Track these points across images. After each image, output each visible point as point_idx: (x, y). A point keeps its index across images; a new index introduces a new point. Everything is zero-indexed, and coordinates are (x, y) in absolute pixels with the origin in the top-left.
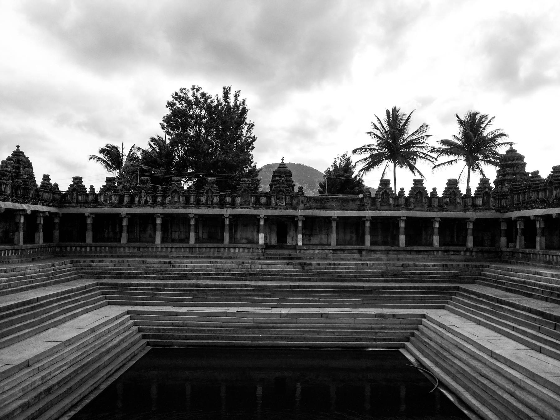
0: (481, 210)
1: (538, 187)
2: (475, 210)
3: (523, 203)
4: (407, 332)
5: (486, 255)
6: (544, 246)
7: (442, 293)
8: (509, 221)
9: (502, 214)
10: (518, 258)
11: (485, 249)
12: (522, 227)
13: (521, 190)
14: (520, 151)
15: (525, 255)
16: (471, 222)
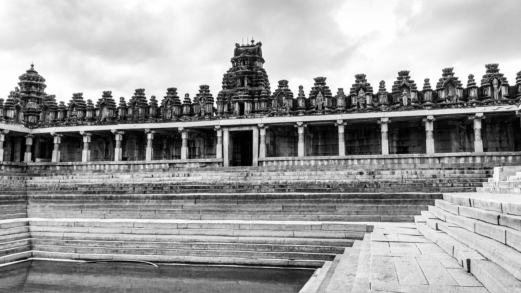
0: (12, 122)
1: (87, 107)
2: (7, 122)
3: (63, 120)
4: (24, 241)
5: (13, 169)
6: (89, 158)
7: (16, 203)
8: (36, 137)
9: (30, 130)
10: (55, 171)
11: (13, 164)
12: (59, 142)
13: (60, 108)
14: (41, 73)
15: (66, 168)
16: (3, 134)
